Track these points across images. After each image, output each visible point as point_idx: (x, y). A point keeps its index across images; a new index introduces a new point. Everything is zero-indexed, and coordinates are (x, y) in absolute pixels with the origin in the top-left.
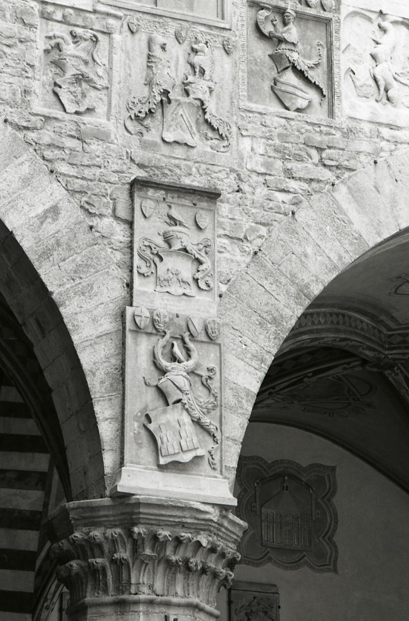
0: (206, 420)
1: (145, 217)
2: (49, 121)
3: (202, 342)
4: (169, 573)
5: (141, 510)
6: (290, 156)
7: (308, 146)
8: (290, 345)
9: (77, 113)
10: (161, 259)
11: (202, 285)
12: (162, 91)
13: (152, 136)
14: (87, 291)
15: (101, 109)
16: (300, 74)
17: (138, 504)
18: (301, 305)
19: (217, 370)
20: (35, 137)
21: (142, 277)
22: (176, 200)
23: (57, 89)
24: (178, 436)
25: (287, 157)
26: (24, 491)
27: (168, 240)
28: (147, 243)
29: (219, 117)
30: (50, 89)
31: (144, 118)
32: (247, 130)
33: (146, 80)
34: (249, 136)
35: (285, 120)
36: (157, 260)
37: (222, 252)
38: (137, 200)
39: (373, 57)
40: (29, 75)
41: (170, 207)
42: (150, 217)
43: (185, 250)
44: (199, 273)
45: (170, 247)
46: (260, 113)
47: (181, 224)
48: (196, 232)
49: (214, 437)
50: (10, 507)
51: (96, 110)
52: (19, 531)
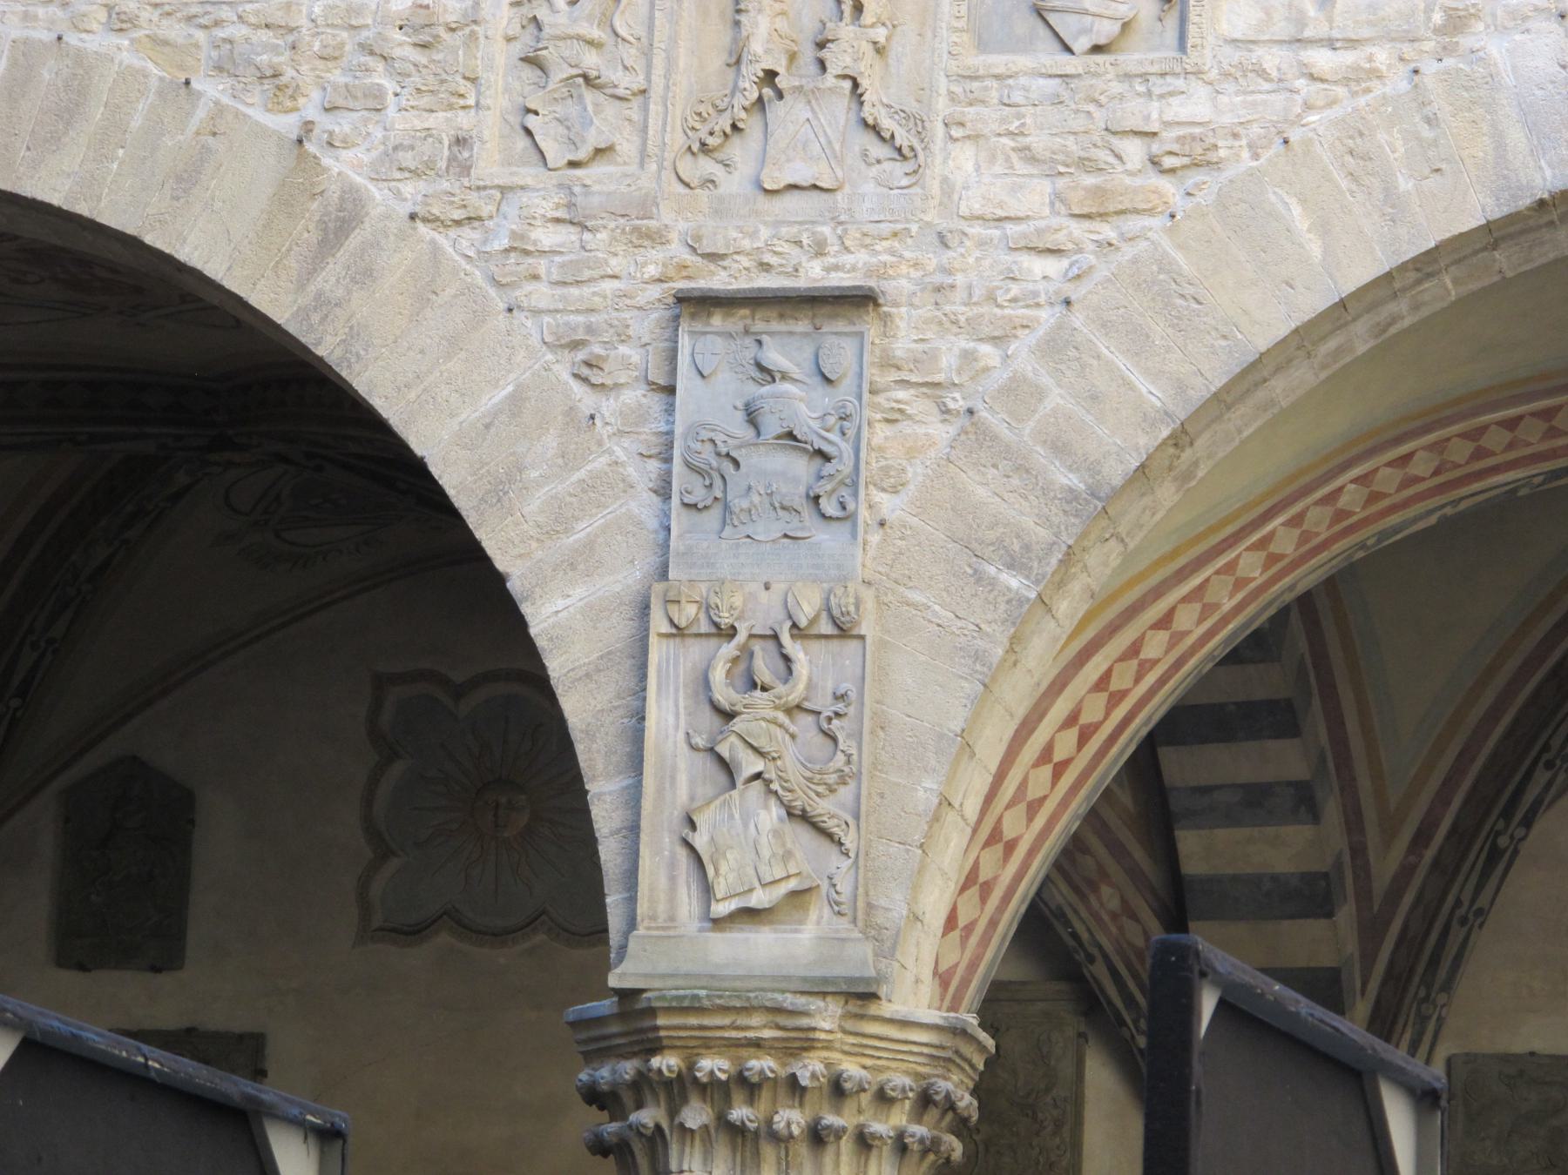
0: (823, 807)
1: (703, 376)
2: (510, 195)
3: (826, 637)
4: (743, 1145)
5: (660, 1021)
6: (1067, 166)
7: (1115, 133)
8: (1443, 506)
9: (573, 164)
10: (736, 463)
11: (830, 507)
12: (761, 74)
13: (734, 184)
14: (580, 562)
15: (627, 146)
17: (652, 1012)
18: (1076, 516)
19: (853, 695)
20: (558, 206)
21: (694, 512)
22: (776, 326)
23: (531, 121)
24: (753, 855)
25: (1062, 169)
26: (1270, 831)
27: (752, 417)
28: (705, 435)
29: (898, 107)
30: (515, 120)
31: (721, 145)
32: (962, 124)
33: (730, 54)
34: (968, 137)
35: (1058, 81)
36: (728, 467)
37: (896, 421)
38: (684, 342)
40: (471, 101)
41: (760, 342)
42: (714, 372)
43: (790, 435)
44: (823, 482)
45: (759, 434)
46: (997, 77)
47: (785, 377)
48: (820, 389)
49: (841, 844)
50: (1249, 871)
51: (618, 148)
52: (1286, 923)
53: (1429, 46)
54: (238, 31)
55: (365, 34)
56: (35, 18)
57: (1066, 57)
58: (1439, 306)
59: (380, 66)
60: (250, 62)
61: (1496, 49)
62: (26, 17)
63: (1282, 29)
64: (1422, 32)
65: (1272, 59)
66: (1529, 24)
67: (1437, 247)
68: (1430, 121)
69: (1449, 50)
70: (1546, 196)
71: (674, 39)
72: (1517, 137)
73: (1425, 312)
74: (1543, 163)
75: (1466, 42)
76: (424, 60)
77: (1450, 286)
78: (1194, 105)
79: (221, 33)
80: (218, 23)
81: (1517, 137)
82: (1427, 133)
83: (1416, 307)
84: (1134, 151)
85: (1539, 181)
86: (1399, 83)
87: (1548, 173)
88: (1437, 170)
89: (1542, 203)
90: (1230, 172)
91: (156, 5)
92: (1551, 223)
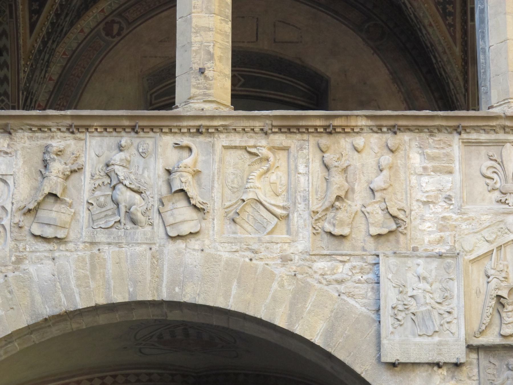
53: (10, 268)
58: (14, 352)
61: (32, 269)
64: (8, 263)
66: (43, 261)
67: (11, 333)
68: (10, 292)
70: (47, 317)
72: (38, 298)
73: (9, 354)
74: (46, 306)
75: (22, 267)
77: (17, 346)
81: (38, 298)
82: (9, 296)
83: (6, 353)
85: (45, 312)
87: (48, 310)
88: (12, 308)
89: (46, 319)
92: (49, 326)
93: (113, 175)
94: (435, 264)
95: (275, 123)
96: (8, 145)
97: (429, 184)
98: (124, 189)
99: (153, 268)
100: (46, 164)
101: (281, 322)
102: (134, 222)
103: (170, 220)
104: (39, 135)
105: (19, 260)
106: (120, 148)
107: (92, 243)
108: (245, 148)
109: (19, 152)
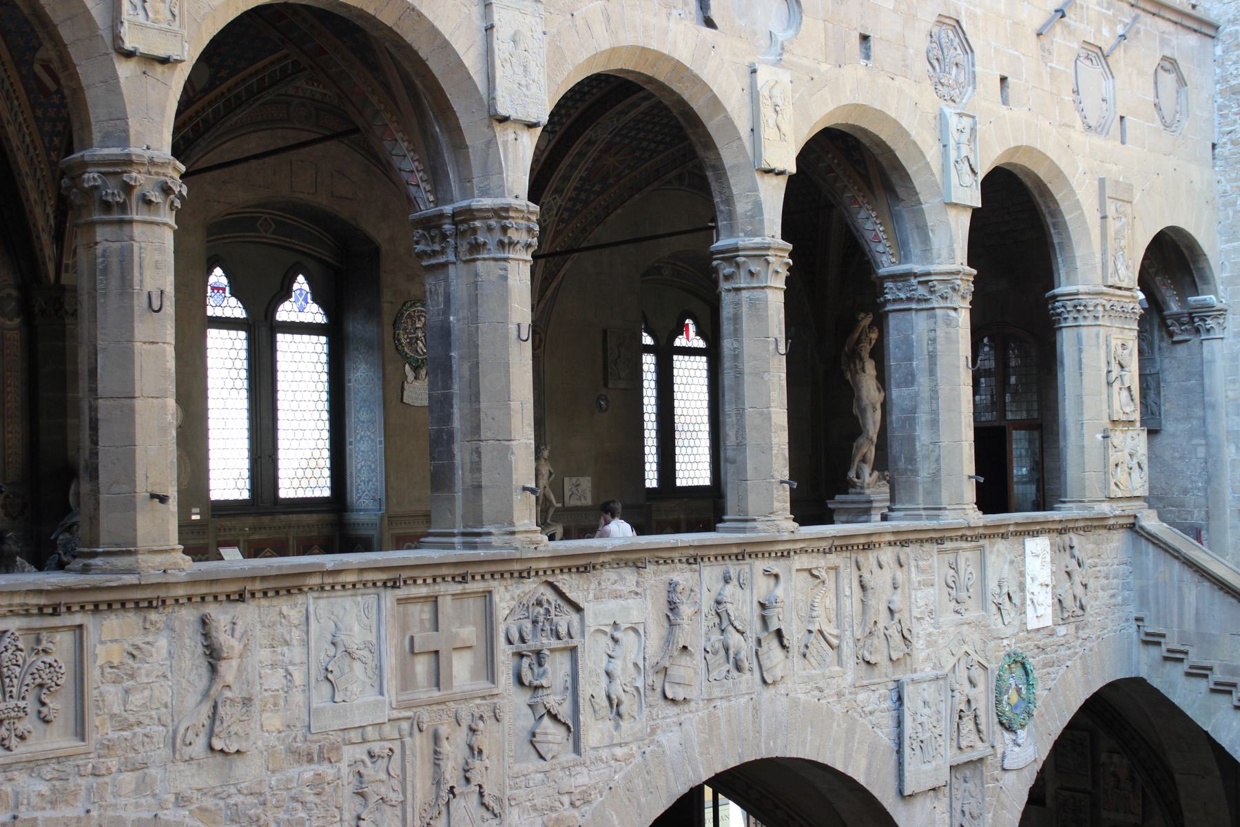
16: (554, 717)
39: (608, 674)
54: (238, 799)
55: (294, 791)
56: (142, 805)
57: (542, 762)
59: (299, 806)
60: (245, 814)
62: (137, 805)
63: (607, 741)
65: (604, 753)
69: (652, 742)
71: (414, 775)
75: (656, 738)
76: (318, 801)
78: (583, 779)
79: (232, 801)
80: (229, 796)
84: (566, 799)
86: (638, 759)
90: (595, 804)
91: (198, 790)
93: (724, 616)
94: (933, 686)
95: (836, 543)
96: (637, 583)
97: (924, 597)
98: (733, 631)
99: (754, 722)
100: (673, 606)
101: (840, 768)
102: (739, 668)
103: (766, 663)
104: (663, 567)
105: (653, 731)
106: (727, 580)
107: (710, 700)
108: (810, 571)
109: (648, 592)
